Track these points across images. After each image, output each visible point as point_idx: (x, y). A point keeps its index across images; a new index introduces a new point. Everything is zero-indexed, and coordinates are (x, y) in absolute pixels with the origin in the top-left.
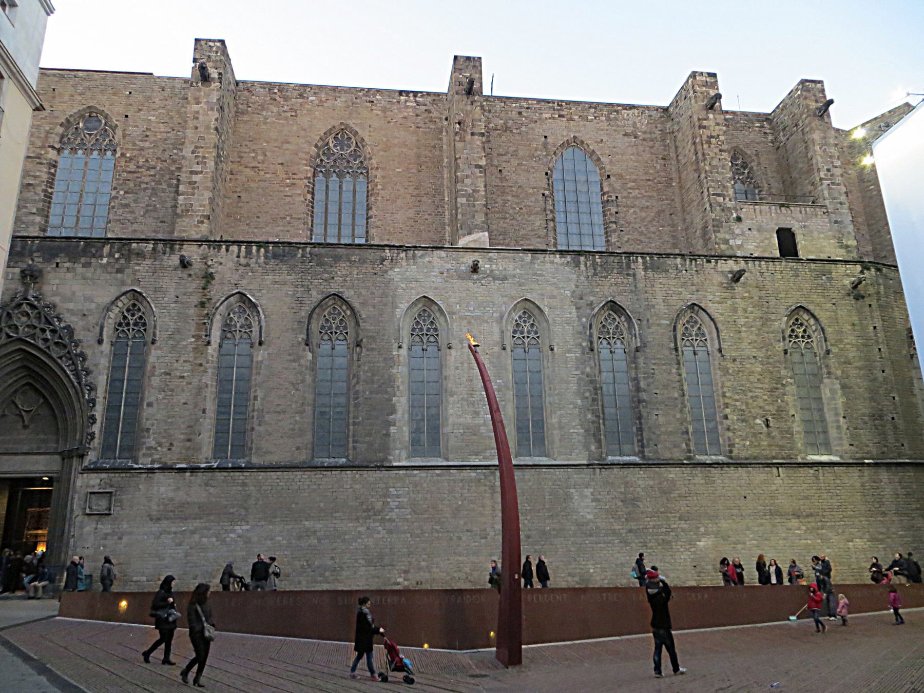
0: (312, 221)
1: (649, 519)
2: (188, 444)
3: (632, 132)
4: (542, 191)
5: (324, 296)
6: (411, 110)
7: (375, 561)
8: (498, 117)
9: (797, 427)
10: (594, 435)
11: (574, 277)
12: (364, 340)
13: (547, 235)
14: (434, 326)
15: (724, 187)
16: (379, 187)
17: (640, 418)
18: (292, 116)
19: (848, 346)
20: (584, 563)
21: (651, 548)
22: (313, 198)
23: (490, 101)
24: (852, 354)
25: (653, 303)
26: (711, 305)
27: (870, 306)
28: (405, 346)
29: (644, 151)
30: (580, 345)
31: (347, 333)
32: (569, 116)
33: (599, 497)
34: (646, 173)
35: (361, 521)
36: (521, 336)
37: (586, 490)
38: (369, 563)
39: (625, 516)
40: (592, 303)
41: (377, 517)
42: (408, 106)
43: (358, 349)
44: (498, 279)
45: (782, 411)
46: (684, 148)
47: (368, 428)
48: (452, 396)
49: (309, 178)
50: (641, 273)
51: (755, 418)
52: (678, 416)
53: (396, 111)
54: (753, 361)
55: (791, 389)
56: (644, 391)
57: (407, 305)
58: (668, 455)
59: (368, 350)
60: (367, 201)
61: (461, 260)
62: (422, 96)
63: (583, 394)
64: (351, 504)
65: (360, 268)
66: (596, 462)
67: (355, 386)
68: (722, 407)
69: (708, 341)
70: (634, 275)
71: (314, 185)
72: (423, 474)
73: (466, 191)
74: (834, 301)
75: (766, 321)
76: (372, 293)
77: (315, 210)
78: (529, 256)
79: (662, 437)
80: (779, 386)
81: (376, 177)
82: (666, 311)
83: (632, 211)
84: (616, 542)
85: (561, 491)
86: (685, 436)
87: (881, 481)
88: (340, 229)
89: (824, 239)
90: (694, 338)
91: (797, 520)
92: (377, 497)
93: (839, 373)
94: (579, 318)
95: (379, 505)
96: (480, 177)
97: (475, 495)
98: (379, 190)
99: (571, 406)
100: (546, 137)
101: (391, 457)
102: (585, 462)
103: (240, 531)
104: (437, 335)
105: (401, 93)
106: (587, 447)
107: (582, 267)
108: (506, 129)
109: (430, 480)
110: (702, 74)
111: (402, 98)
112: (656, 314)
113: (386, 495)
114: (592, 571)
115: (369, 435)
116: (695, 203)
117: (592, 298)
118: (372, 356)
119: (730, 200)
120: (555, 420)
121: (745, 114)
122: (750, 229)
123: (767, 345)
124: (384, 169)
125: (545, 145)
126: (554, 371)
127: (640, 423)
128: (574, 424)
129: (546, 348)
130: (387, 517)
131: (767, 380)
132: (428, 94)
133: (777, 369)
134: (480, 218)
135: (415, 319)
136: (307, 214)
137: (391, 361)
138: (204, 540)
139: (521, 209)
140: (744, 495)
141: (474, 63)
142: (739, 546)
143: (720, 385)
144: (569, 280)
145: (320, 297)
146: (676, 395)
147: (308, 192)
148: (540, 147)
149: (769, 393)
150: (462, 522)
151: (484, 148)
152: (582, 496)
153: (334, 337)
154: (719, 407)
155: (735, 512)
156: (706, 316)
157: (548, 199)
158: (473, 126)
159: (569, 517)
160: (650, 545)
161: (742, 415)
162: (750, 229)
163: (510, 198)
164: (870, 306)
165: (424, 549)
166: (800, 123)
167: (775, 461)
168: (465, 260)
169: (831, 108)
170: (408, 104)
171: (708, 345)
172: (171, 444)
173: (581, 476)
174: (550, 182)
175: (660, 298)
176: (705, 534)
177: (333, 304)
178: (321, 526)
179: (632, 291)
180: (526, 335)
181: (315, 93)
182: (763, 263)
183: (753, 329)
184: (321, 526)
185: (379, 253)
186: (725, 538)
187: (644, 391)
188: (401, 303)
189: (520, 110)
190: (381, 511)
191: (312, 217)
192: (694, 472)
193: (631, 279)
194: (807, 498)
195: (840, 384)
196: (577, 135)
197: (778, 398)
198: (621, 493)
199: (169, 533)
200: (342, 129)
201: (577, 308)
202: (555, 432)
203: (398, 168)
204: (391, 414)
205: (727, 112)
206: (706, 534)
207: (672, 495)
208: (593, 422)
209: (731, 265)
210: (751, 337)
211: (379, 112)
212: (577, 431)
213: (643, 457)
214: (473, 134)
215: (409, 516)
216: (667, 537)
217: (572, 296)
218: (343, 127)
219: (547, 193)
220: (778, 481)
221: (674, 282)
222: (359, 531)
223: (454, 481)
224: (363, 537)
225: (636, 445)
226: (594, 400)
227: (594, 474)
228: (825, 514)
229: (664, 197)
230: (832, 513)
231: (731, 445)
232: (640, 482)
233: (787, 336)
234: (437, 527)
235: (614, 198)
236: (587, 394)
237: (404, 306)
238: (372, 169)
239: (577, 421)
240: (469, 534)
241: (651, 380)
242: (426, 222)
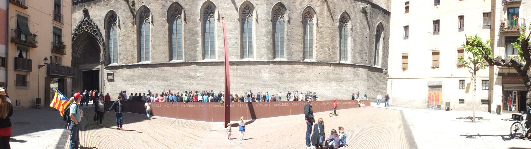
1: (287, 80)
2: (132, 57)
30: (267, 18)
37: (266, 70)
52: (300, 45)
58: (295, 59)
95: (193, 75)
103: (150, 84)
112: (296, 9)
117: (272, 1)
138: (139, 86)
145: (171, 3)
146: (300, 38)
160: (287, 88)
172: (127, 58)
178: (175, 82)
184: (175, 82)
188: (200, 3)
199: (129, 84)
201: (267, 4)
206: (305, 85)
207: (296, 72)
208: (270, 46)
226: (271, 39)
236: (269, 36)
239: (264, 46)
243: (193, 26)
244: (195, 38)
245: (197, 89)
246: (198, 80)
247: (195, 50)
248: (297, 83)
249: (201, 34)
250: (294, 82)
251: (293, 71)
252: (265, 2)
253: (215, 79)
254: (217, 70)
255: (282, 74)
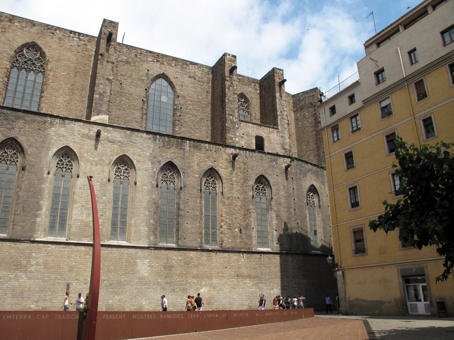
0: (6, 94)
1: (177, 277)
3: (193, 76)
4: (142, 98)
5: (6, 138)
6: (75, 42)
7: (18, 295)
8: (124, 55)
9: (254, 234)
10: (153, 232)
11: (152, 146)
12: (27, 166)
13: (142, 122)
14: (71, 163)
15: (234, 111)
16: (50, 81)
17: (178, 224)
18: (2, 31)
19: (281, 196)
20: (140, 299)
21: (177, 292)
22: (8, 80)
23: (121, 46)
24: (283, 200)
25: (192, 165)
26: (220, 169)
27: (292, 178)
28: (52, 173)
29: (198, 87)
31: (17, 161)
32: (162, 62)
33: (152, 264)
34: (197, 98)
35: (12, 271)
36: (119, 174)
37: (145, 260)
38: (13, 296)
39: (165, 275)
40: (160, 162)
41: (22, 270)
42: (74, 40)
43: (23, 172)
44: (110, 142)
45: (248, 225)
46: (217, 89)
47: (23, 217)
48: (76, 203)
49: (8, 69)
50: (187, 148)
51: (235, 228)
52: (198, 224)
53: (67, 41)
54: (238, 200)
55: (254, 215)
56: (182, 210)
57: (56, 150)
59: (29, 172)
60: (42, 87)
61: (91, 128)
62: (83, 36)
63: (150, 209)
64: (7, 261)
65: (30, 125)
66: (152, 246)
67: (18, 192)
68: (220, 222)
69: (217, 187)
70: (184, 149)
71: (10, 73)
72: (54, 246)
73: (99, 91)
74: (277, 174)
75: (246, 180)
76: (36, 140)
77: (9, 88)
78: (129, 132)
79: (188, 235)
80: (248, 213)
81: (49, 75)
82: (198, 170)
83: (188, 116)
84: (158, 288)
85: (132, 261)
86: (200, 235)
87: (288, 262)
88: (22, 101)
89: (276, 144)
90: (211, 185)
91: (249, 279)
92: (24, 257)
93: (276, 209)
94: (153, 168)
95: (24, 262)
96: (108, 85)
97: (83, 260)
98: (50, 82)
99: (143, 215)
100: (148, 70)
101: (36, 236)
102: (147, 246)
104: (72, 168)
105: (71, 32)
106: (148, 237)
107: (158, 142)
108: (128, 62)
109: (57, 250)
110: (229, 55)
111: (71, 34)
113: (30, 257)
114: (144, 303)
115: (24, 222)
116: (219, 117)
117: (160, 159)
118: (31, 176)
119: (236, 118)
120: (133, 222)
121: (248, 78)
122: (243, 134)
123: (245, 193)
124: (54, 71)
125: (147, 75)
126: (135, 195)
127: (178, 227)
128: (143, 225)
129: (132, 183)
130: (29, 270)
131: (243, 210)
132: (87, 35)
133: (248, 205)
134: (105, 108)
135: (60, 158)
136: (3, 89)
137: (41, 180)
139: (129, 106)
140: (226, 266)
141: (115, 25)
142: (221, 292)
143: (220, 210)
144: (149, 147)
146: (198, 214)
147: (6, 77)
148: (144, 75)
149: (243, 216)
150: (74, 275)
151: (113, 70)
152: (143, 264)
153: (8, 162)
154: (219, 221)
155: (220, 274)
156: (218, 175)
157: (145, 103)
158: (109, 58)
159: (135, 274)
160: (176, 290)
161: (229, 226)
162: (243, 134)
163: (124, 99)
164: (292, 178)
165: (49, 289)
166: (271, 87)
167: (242, 250)
168: (94, 129)
169: (285, 83)
170: (74, 39)
171: (217, 190)
173: (143, 253)
174: (147, 94)
175: (196, 163)
176: (204, 285)
177: (11, 143)
179: (181, 158)
180: (122, 174)
181: (19, 21)
182: (247, 152)
183: (239, 183)
185: (44, 118)
186: (214, 288)
187: (182, 210)
188: (53, 148)
189: (136, 54)
190: (25, 266)
191: (6, 91)
192: (203, 254)
193: (182, 151)
194: (255, 268)
195: (276, 214)
196: (165, 72)
197: (247, 219)
198: (164, 263)
200: (33, 45)
201: (152, 163)
202: (132, 228)
203: (63, 72)
204: (39, 210)
205: (240, 75)
206: (205, 285)
207: (190, 265)
208: (153, 225)
209: (232, 151)
210: (238, 188)
211: (57, 40)
212: (144, 229)
213: (178, 244)
214: (108, 62)
215: (43, 270)
216: (185, 287)
217: (150, 156)
218: (33, 44)
219: (145, 99)
220: (243, 260)
221: (203, 155)
222: (10, 277)
223: (72, 251)
224: (12, 280)
225: (175, 238)
226: (155, 213)
227: (151, 252)
228: (262, 276)
229: (205, 111)
230: (265, 276)
231: (222, 241)
232: (175, 258)
233: (254, 189)
234: (58, 277)
235: (180, 108)
236: (152, 209)
237: (55, 150)
238: (47, 70)
239: (145, 223)
240: (77, 281)
241: (186, 205)
242: (75, 104)
243: (36, 182)
244: (37, 200)
245: (28, 287)
246: (31, 272)
247: (33, 220)
248: (192, 283)
249: (47, 196)
250: (187, 280)
251: (187, 264)
252: (149, 159)
253: (61, 271)
254: (67, 257)
255: (169, 268)
